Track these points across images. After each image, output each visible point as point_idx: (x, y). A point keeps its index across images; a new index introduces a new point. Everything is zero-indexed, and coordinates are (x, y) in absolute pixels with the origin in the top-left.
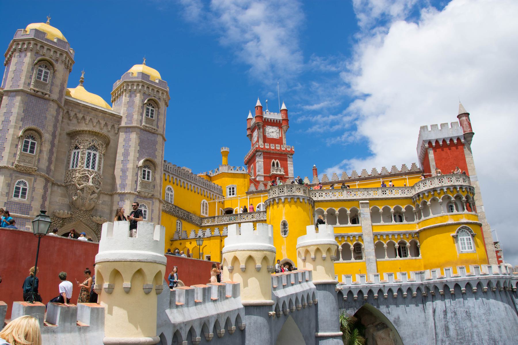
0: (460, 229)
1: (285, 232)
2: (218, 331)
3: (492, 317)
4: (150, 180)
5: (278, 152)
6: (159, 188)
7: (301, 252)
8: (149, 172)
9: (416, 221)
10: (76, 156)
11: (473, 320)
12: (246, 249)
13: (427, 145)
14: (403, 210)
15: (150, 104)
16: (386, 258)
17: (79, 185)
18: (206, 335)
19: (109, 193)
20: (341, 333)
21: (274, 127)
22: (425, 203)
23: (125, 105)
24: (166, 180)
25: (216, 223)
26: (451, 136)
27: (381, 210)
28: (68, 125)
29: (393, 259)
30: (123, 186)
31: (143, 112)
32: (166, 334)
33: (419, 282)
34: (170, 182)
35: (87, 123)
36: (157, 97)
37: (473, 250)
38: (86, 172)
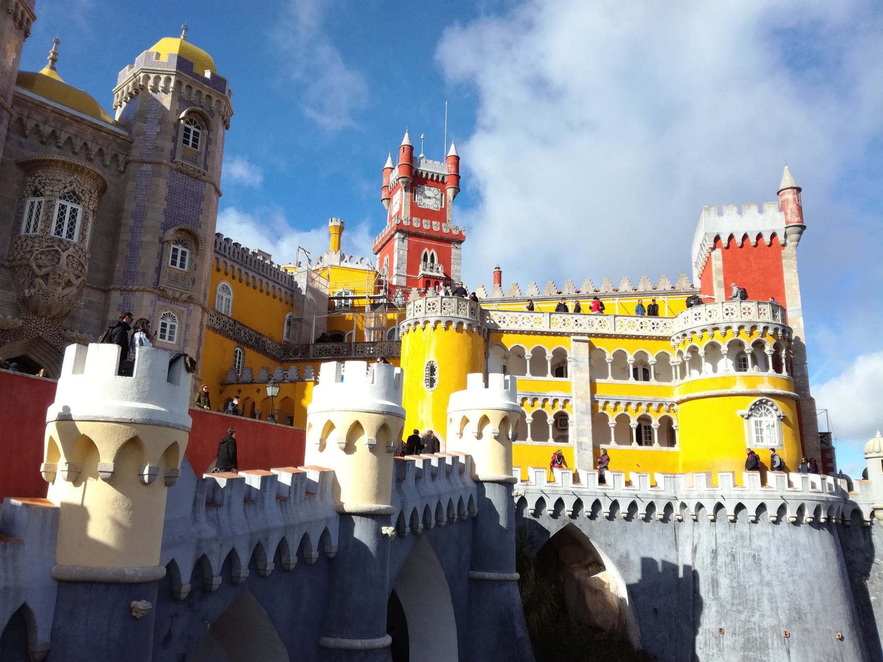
0: (755, 404)
1: (432, 382)
2: (284, 559)
9: (676, 382)
10: (35, 210)
11: (764, 572)
15: (191, 120)
18: (261, 567)
19: (103, 287)
20: (517, 576)
21: (432, 189)
22: (693, 350)
24: (218, 270)
25: (311, 357)
29: (625, 447)
32: (179, 562)
35: (61, 145)
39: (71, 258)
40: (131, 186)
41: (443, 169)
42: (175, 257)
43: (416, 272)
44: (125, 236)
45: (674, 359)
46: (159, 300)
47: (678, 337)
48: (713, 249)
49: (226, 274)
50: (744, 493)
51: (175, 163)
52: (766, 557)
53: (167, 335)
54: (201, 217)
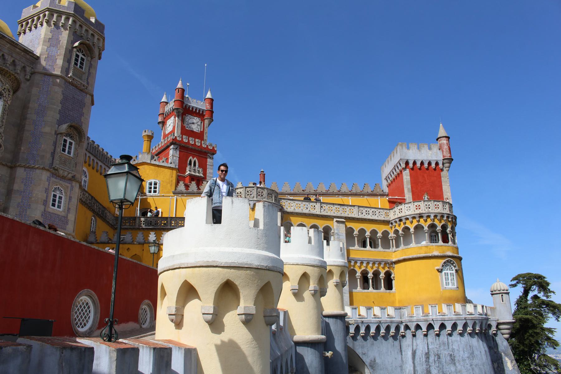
0: (445, 263)
3: (475, 362)
4: (72, 155)
5: (197, 149)
8: (71, 144)
11: (457, 364)
12: (300, 262)
13: (403, 165)
14: (379, 235)
15: (80, 49)
19: (9, 164)
21: (195, 118)
22: (406, 229)
23: (44, 41)
25: (137, 227)
26: (430, 159)
33: (397, 319)
37: (456, 287)
40: (35, 91)
41: (203, 106)
42: (65, 146)
43: (185, 171)
45: (392, 235)
46: (53, 177)
47: (396, 222)
48: (405, 169)
50: (446, 317)
52: (458, 355)
53: (57, 203)
54: (82, 118)
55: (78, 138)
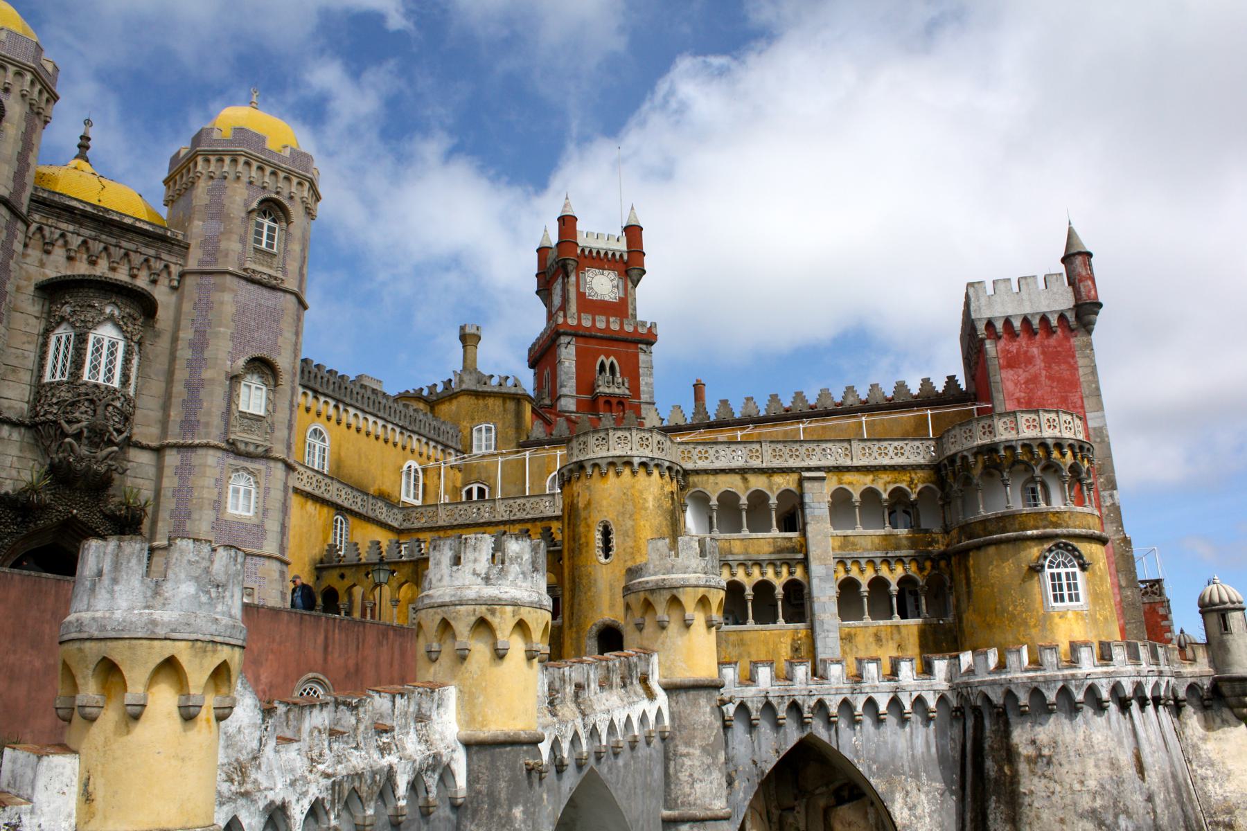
0: (1050, 550)
1: (607, 550)
6: (286, 432)
7: (633, 606)
10: (62, 348)
16: (867, 620)
17: (69, 422)
26: (1044, 309)
27: (856, 497)
28: (42, 264)
29: (881, 622)
30: (189, 426)
31: (246, 232)
34: (319, 414)
36: (285, 192)
38: (89, 391)
39: (110, 409)
40: (187, 307)
44: (181, 374)
49: (319, 414)
51: (245, 270)
55: (271, 379)
